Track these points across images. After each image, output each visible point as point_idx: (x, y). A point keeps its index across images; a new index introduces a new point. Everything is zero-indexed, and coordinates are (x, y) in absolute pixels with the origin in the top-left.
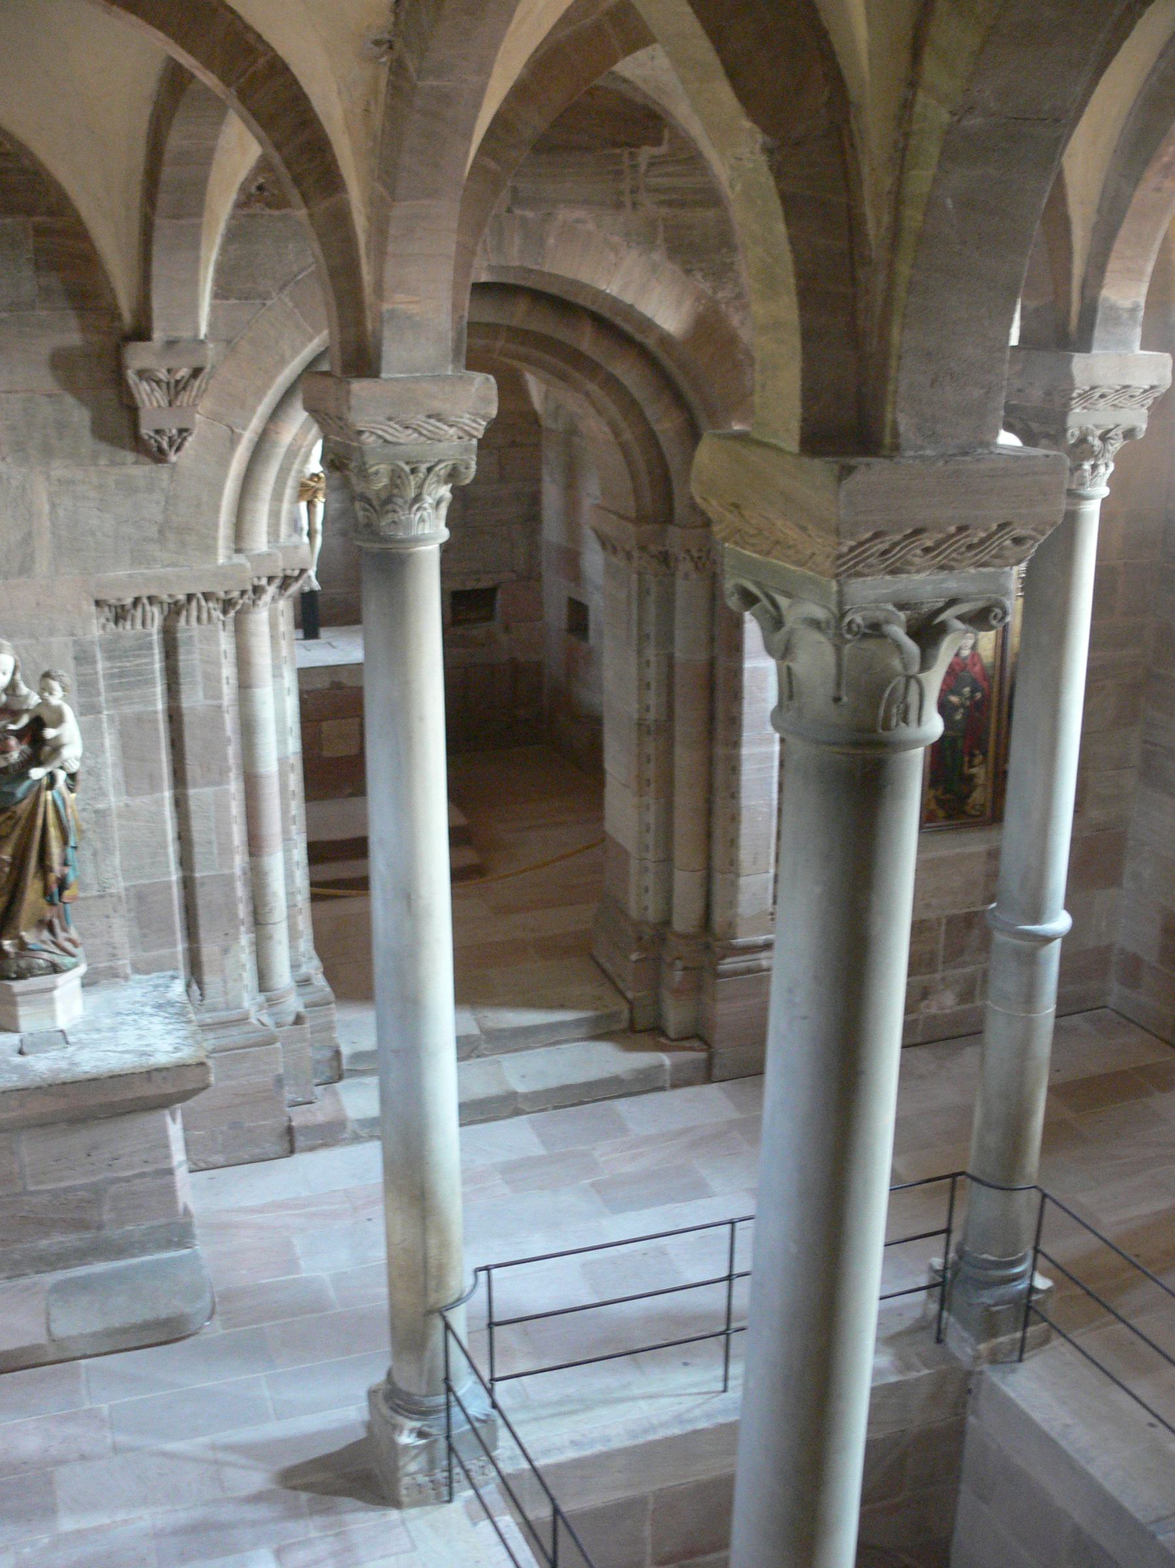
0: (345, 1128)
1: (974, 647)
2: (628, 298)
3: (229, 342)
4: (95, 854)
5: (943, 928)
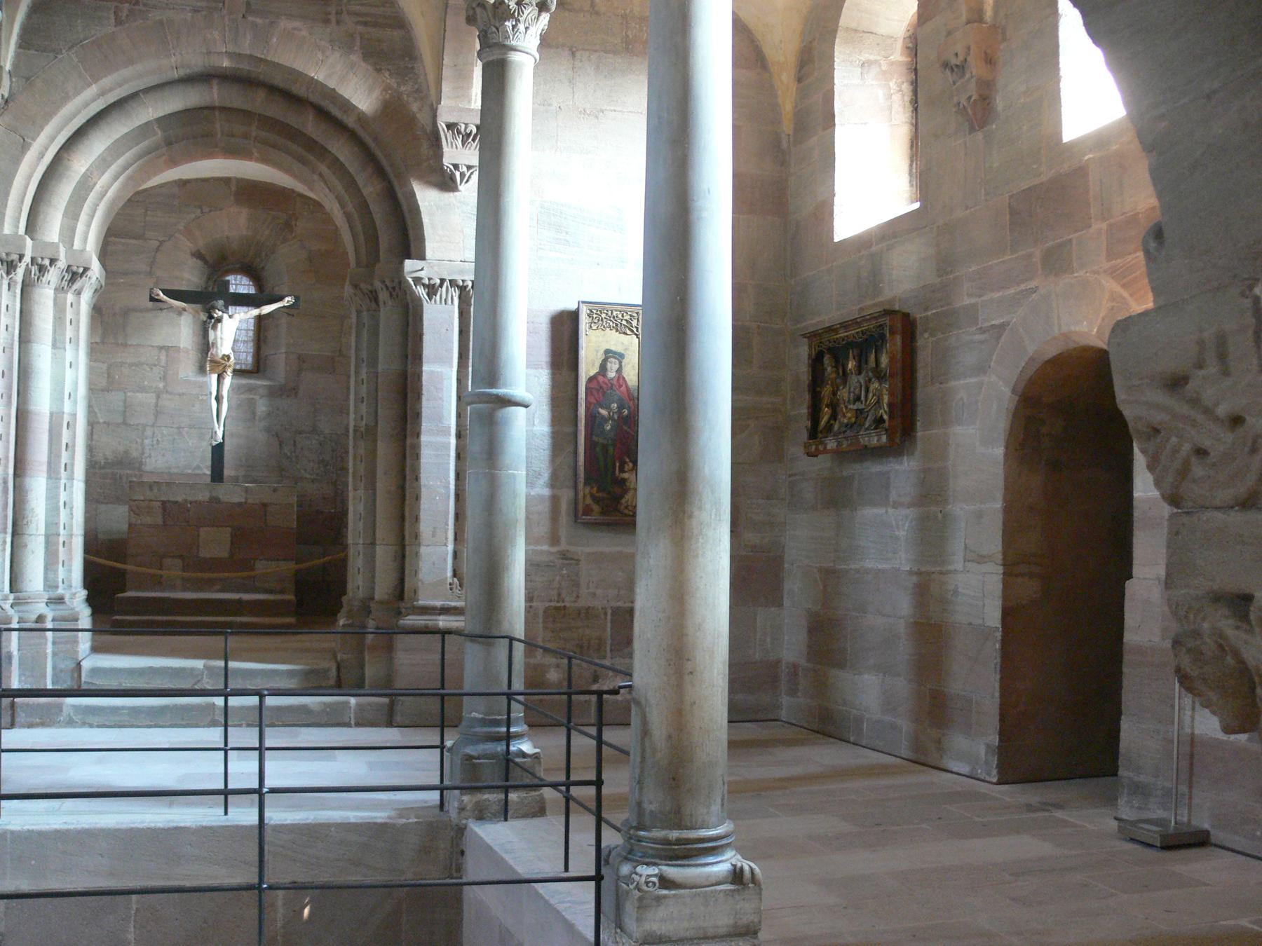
0: (61, 711)
1: (619, 371)
2: (332, 84)
5: (609, 618)
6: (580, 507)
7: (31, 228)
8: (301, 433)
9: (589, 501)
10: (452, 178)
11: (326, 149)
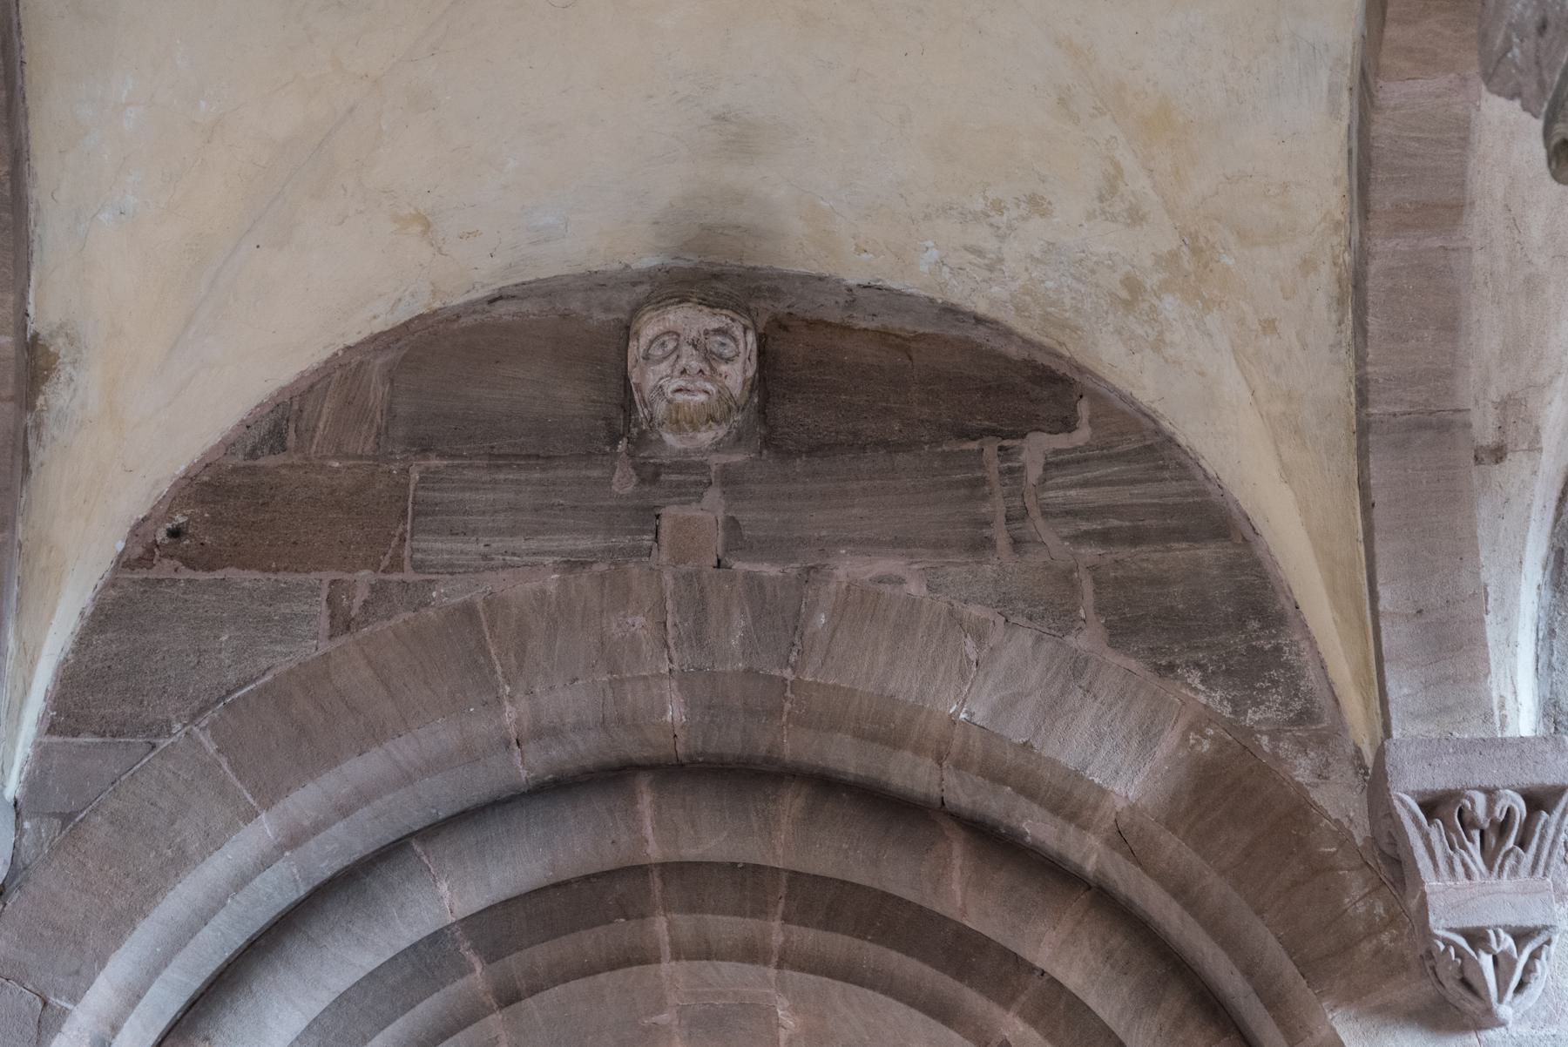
3: (66, 818)
10: (1470, 985)
11: (1018, 960)
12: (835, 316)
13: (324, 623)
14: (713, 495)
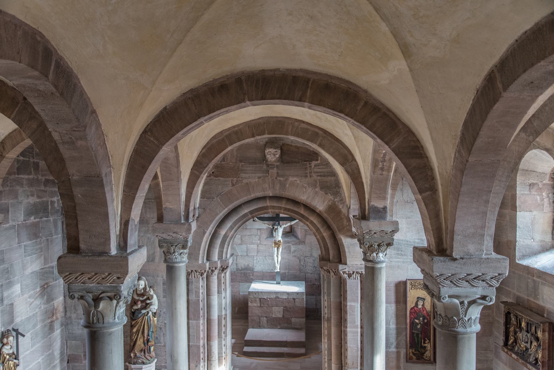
1: (423, 305)
4: (164, 334)
6: (408, 357)
7: (208, 260)
8: (307, 257)
9: (411, 354)
12: (290, 144)
13: (231, 185)
14: (275, 169)
